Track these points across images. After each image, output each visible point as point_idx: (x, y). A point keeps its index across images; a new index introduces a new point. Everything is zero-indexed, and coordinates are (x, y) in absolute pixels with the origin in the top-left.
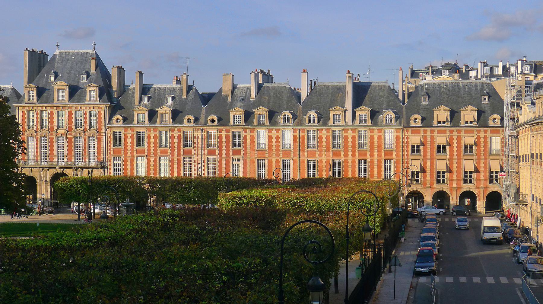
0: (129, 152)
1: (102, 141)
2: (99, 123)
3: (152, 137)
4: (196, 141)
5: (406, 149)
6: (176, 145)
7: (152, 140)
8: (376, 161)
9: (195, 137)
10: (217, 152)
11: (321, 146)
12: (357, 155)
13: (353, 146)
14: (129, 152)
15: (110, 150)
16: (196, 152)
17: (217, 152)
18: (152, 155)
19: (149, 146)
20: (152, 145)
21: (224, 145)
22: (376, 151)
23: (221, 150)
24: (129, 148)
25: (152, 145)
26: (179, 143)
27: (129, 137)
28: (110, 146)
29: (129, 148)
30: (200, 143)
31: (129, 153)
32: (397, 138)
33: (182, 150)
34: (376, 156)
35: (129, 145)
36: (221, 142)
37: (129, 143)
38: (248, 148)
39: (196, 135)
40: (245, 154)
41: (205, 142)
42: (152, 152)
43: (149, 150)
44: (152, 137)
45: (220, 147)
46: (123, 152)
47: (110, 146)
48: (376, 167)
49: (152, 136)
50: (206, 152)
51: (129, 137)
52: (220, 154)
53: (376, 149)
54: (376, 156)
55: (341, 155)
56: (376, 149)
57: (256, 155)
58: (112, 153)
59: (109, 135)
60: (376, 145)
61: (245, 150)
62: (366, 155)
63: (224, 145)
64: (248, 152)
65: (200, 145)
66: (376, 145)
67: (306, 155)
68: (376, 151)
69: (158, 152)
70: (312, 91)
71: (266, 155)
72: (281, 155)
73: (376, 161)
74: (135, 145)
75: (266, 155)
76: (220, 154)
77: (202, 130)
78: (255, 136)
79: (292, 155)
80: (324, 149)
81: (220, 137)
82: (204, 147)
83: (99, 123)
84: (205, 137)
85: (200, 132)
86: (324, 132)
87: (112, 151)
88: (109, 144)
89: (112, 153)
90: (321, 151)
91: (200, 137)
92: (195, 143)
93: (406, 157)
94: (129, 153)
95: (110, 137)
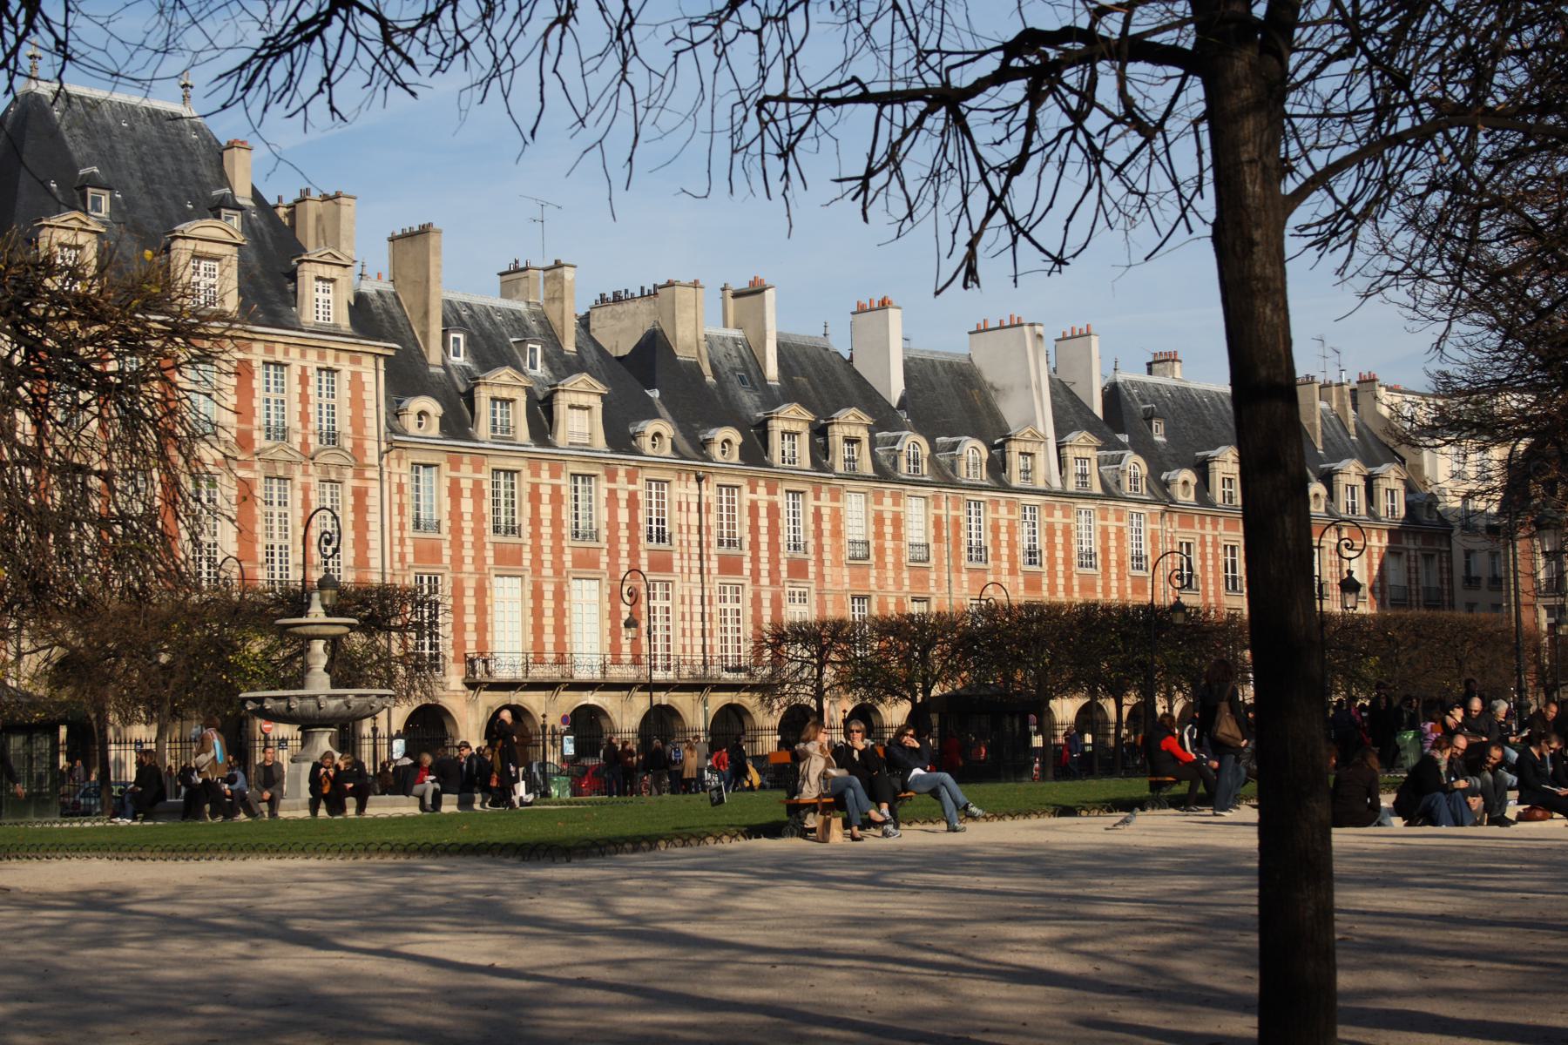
0: (468, 553)
1: (373, 501)
2: (358, 423)
3: (546, 498)
4: (684, 522)
6: (624, 533)
7: (546, 510)
9: (680, 504)
10: (747, 566)
14: (468, 553)
15: (402, 541)
16: (686, 563)
17: (747, 566)
18: (547, 571)
19: (536, 535)
20: (546, 530)
21: (764, 539)
23: (755, 559)
24: (468, 538)
25: (546, 530)
26: (633, 525)
27: (467, 493)
28: (402, 527)
29: (468, 538)
30: (694, 530)
31: (468, 560)
33: (644, 555)
35: (468, 525)
36: (754, 529)
37: (467, 517)
38: (827, 556)
39: (683, 499)
40: (820, 576)
41: (708, 528)
42: (547, 557)
43: (537, 551)
44: (546, 498)
45: (755, 545)
46: (447, 552)
47: (402, 527)
49: (545, 492)
50: (714, 564)
51: (467, 493)
52: (756, 574)
53: (1114, 570)
57: (847, 579)
58: (410, 558)
59: (396, 479)
61: (820, 562)
63: (764, 539)
64: (827, 571)
65: (695, 538)
67: (965, 585)
69: (568, 558)
70: (915, 370)
71: (872, 581)
74: (488, 526)
75: (872, 581)
76: (756, 574)
77: (699, 480)
79: (932, 583)
80: (1005, 565)
81: (754, 509)
82: (709, 545)
83: (358, 423)
84: (708, 505)
85: (693, 485)
86: (1003, 510)
87: (409, 549)
88: (396, 519)
89: (410, 558)
91: (694, 507)
92: (680, 526)
94: (468, 560)
95: (401, 487)
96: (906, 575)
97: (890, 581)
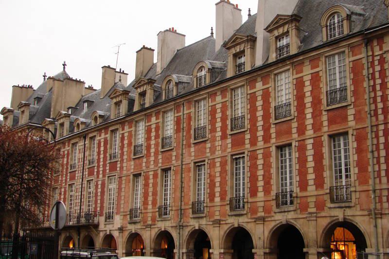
5: (379, 93)
8: (309, 143)
11: (213, 130)
12: (273, 136)
13: (266, 117)
22: (309, 116)
32: (356, 69)
34: (310, 132)
48: (310, 159)
53: (309, 111)
54: (310, 132)
55: (244, 143)
56: (309, 111)
57: (133, 167)
60: (308, 100)
62: (289, 132)
66: (308, 100)
68: (309, 116)
71: (144, 164)
72: (160, 161)
73: (309, 143)
75: (144, 164)
78: (133, 133)
90: (214, 140)
93: (381, 117)
96: (160, 157)
97: (152, 163)
